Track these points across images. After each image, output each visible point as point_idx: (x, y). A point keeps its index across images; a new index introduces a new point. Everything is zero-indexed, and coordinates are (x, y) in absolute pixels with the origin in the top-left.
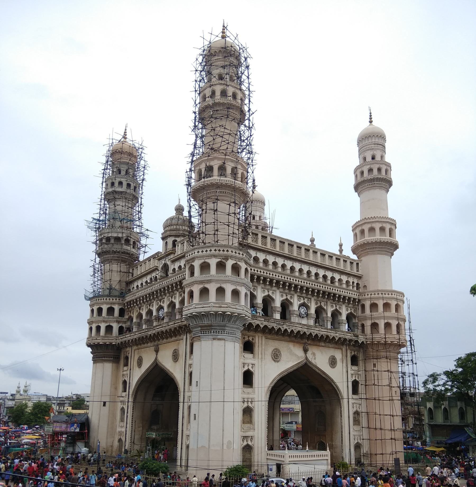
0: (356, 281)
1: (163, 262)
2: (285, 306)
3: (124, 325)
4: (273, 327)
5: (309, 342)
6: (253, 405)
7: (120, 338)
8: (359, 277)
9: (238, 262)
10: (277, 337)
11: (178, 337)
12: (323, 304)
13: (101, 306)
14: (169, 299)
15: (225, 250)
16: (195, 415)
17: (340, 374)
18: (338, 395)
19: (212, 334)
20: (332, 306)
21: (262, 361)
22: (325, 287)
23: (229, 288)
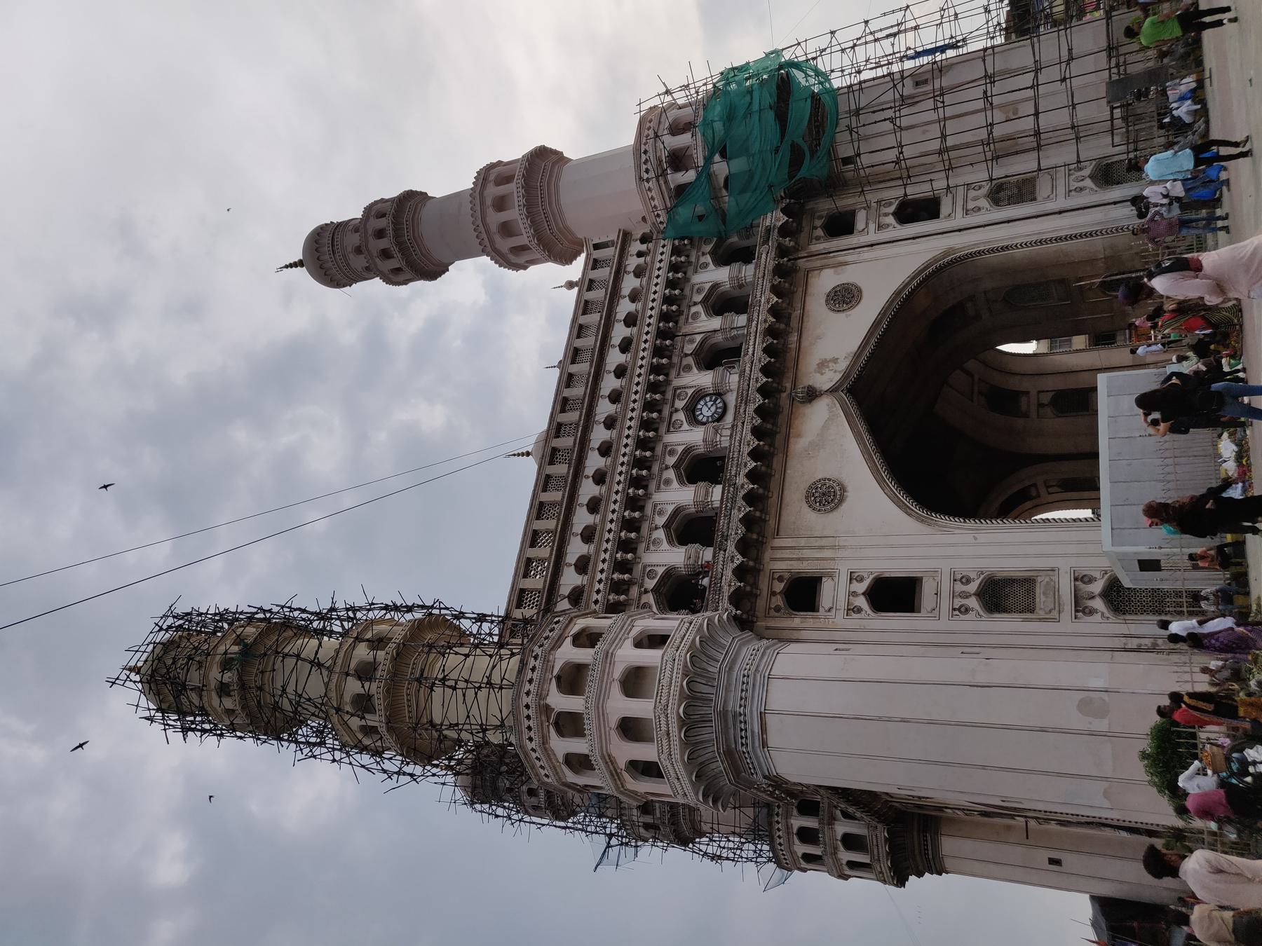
0: (636, 246)
4: (741, 520)
5: (788, 385)
6: (973, 575)
8: (626, 237)
9: (555, 672)
10: (775, 495)
12: (689, 348)
17: (879, 266)
18: (940, 270)
19: (750, 748)
20: (696, 316)
21: (840, 547)
22: (644, 350)
23: (621, 706)
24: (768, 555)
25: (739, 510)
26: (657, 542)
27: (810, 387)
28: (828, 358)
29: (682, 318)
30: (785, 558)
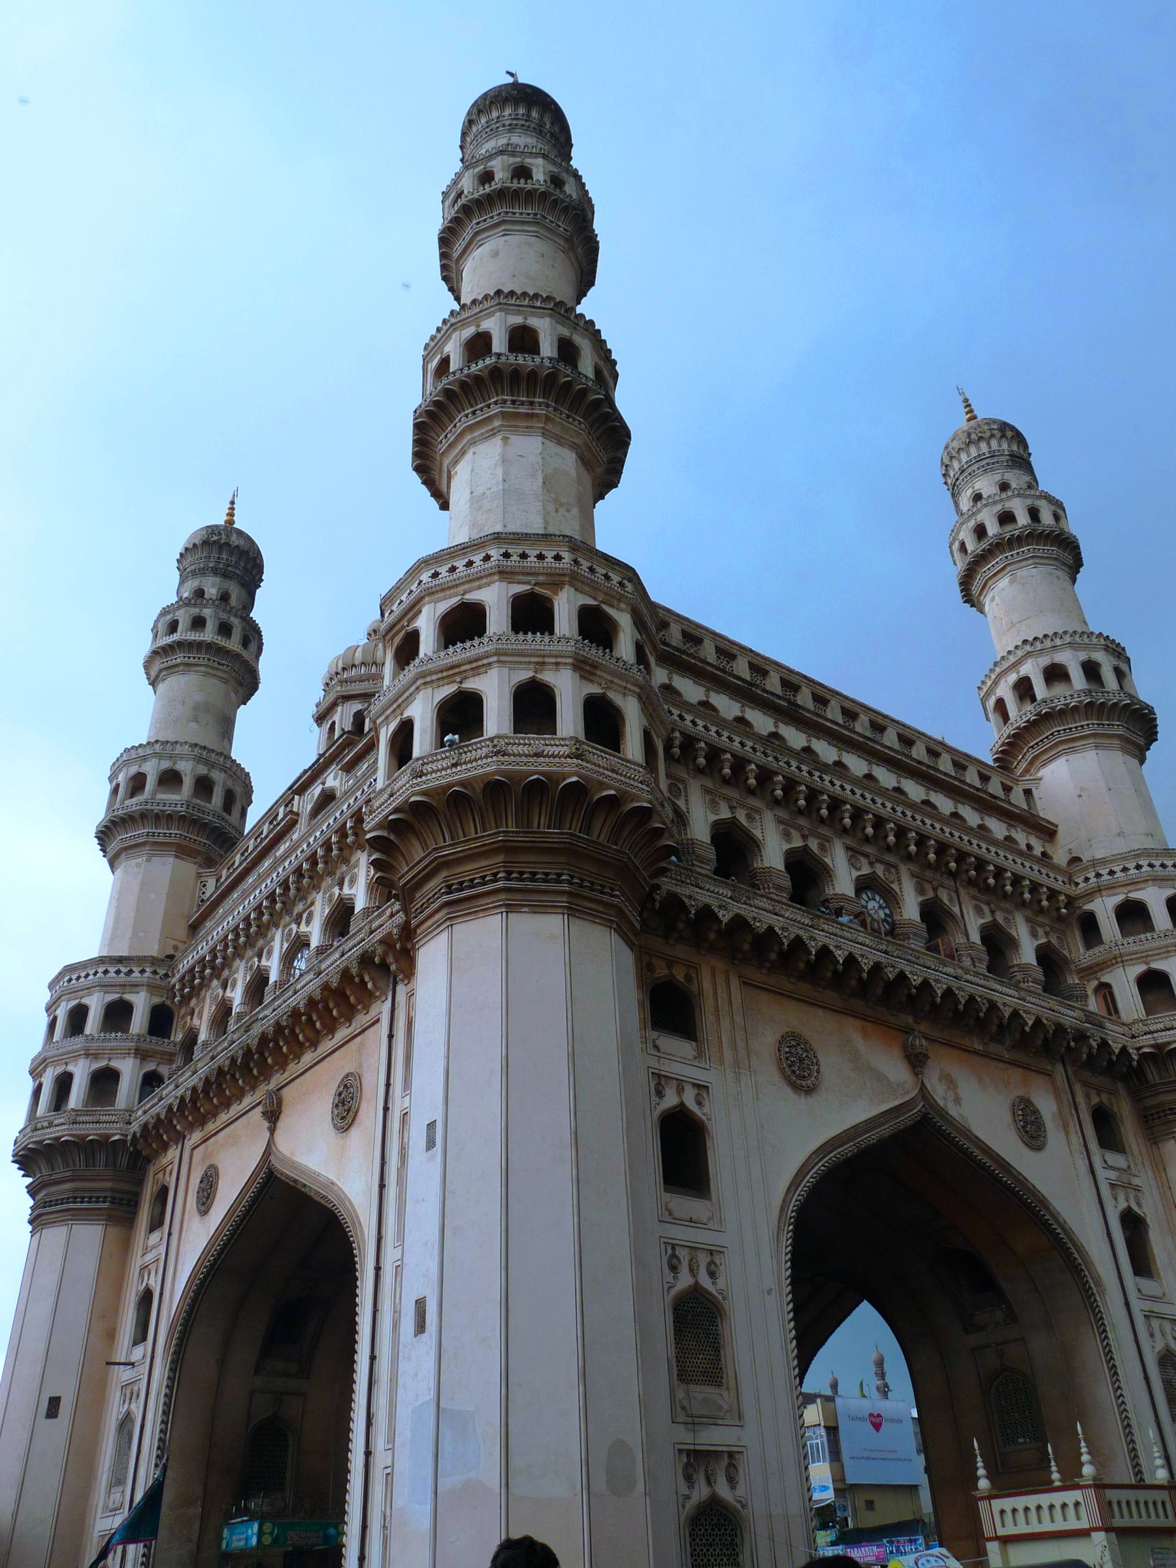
1: (316, 790)
2: (805, 875)
3: (164, 1070)
4: (771, 929)
5: (924, 1027)
6: (721, 1282)
7: (140, 1112)
8: (1048, 832)
9: (604, 607)
11: (361, 1020)
12: (944, 896)
13: (85, 1001)
14: (331, 896)
15: (550, 555)
16: (420, 1305)
20: (979, 911)
24: (720, 965)
25: (783, 929)
26: (714, 806)
27: (926, 1057)
28: (960, 1091)
29: (974, 892)
30: (717, 990)
